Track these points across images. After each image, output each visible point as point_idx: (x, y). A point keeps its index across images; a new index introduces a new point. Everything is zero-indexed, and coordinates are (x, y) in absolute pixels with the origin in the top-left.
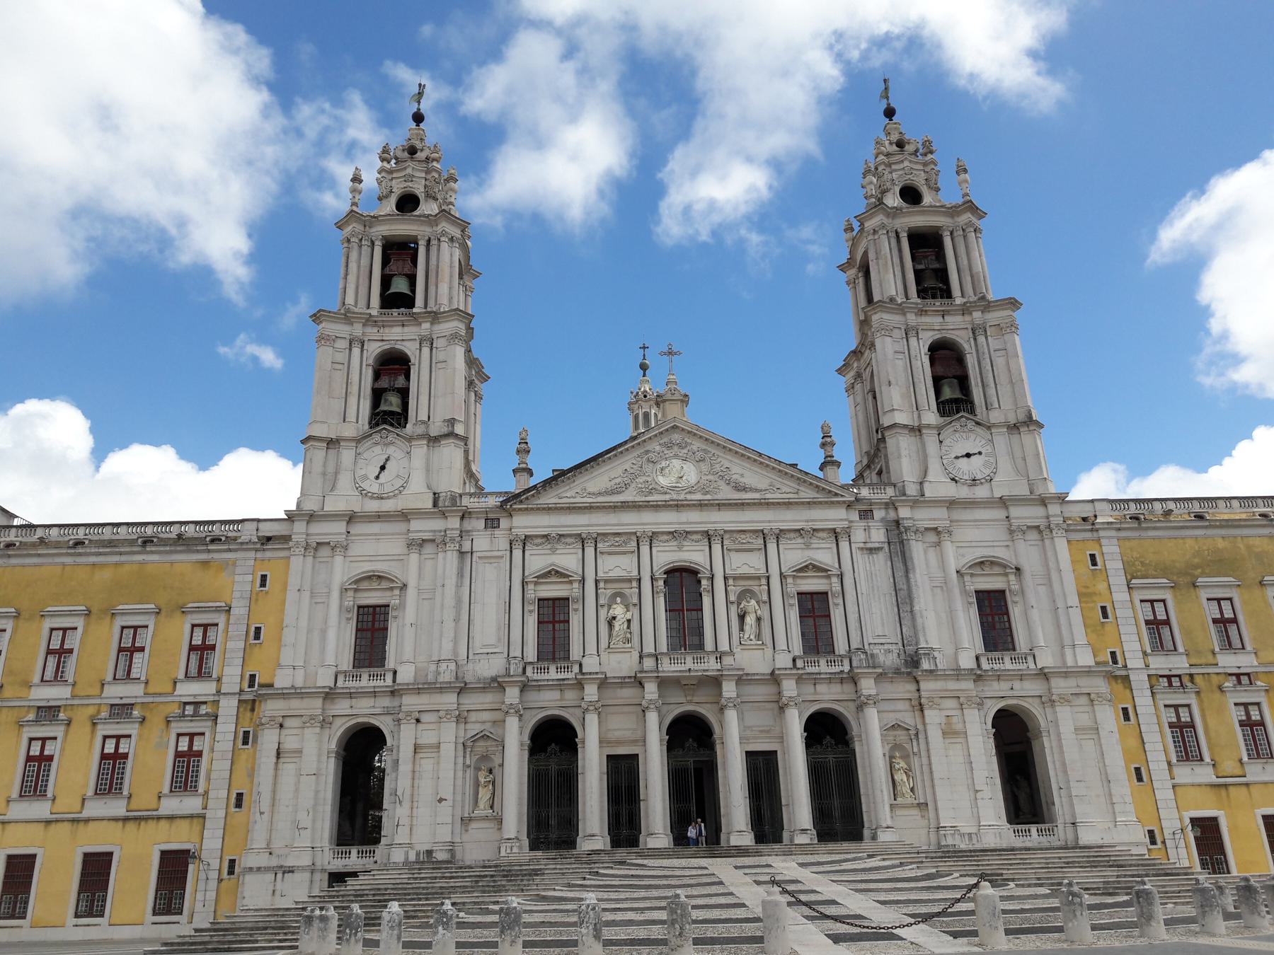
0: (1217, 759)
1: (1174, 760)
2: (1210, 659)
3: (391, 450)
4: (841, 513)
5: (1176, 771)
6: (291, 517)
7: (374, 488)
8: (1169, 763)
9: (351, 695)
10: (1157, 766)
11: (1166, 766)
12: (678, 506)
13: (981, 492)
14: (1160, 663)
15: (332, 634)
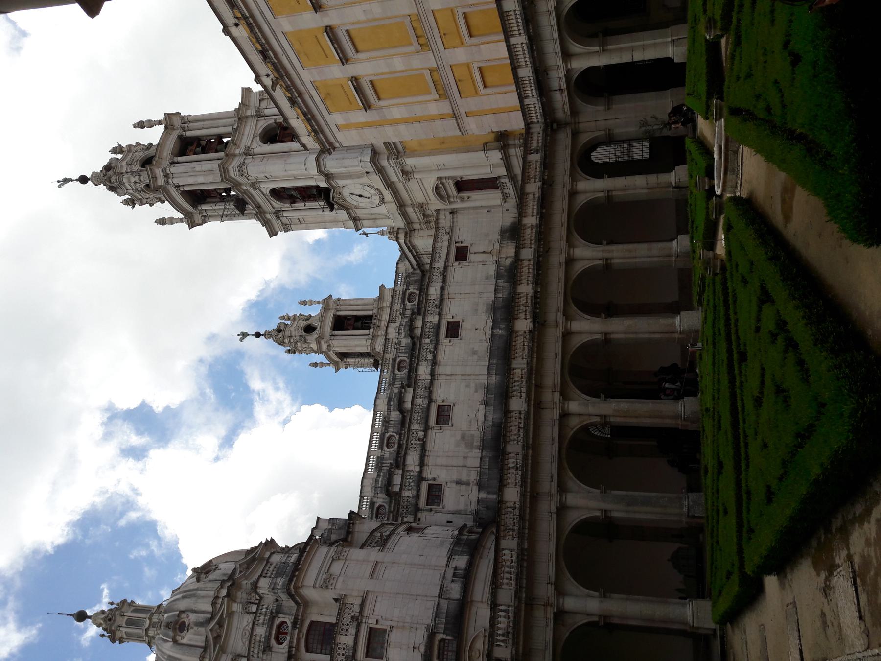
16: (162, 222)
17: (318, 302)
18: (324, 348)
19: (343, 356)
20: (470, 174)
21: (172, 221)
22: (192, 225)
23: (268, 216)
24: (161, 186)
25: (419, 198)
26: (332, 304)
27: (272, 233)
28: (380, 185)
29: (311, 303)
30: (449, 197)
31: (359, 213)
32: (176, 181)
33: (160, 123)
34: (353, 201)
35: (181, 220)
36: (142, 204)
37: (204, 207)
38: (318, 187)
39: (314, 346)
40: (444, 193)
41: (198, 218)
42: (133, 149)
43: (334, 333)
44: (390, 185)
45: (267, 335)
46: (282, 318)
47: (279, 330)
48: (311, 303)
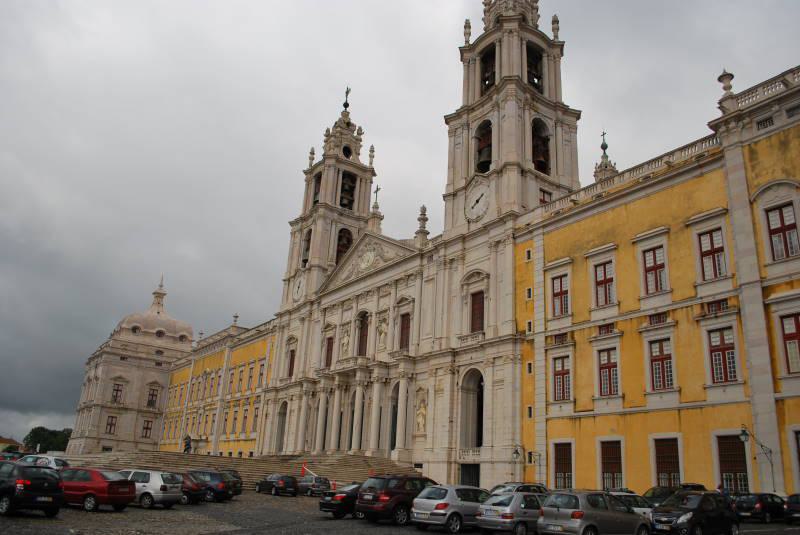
0: (578, 397)
1: (551, 400)
2: (585, 316)
3: (302, 279)
4: (417, 262)
5: (551, 408)
6: (280, 315)
7: (296, 298)
8: (547, 404)
9: (282, 390)
10: (540, 406)
11: (544, 404)
12: (370, 276)
13: (480, 225)
14: (555, 327)
15: (282, 362)
16: (467, 26)
17: (371, 163)
18: (328, 162)
19: (318, 178)
20: (489, 306)
21: (467, 34)
22: (462, 50)
23: (465, 116)
24: (502, 26)
25: (471, 256)
26: (368, 175)
27: (448, 119)
28: (486, 220)
29: (372, 157)
30: (468, 285)
31: (461, 198)
32: (505, 39)
33: (556, 36)
34: (474, 194)
35: (467, 42)
36: (485, 12)
37: (478, 62)
38: (490, 162)
39: (331, 152)
40: (473, 280)
41: (467, 55)
42: (534, 11)
43: (341, 173)
44: (486, 228)
45: (345, 114)
46: (360, 129)
47: (349, 124)
48: (372, 157)
